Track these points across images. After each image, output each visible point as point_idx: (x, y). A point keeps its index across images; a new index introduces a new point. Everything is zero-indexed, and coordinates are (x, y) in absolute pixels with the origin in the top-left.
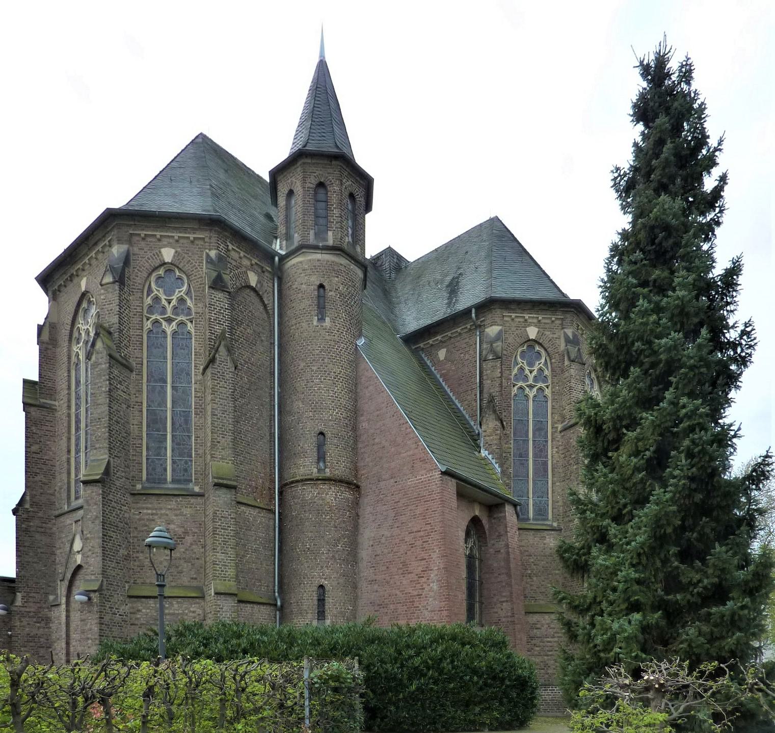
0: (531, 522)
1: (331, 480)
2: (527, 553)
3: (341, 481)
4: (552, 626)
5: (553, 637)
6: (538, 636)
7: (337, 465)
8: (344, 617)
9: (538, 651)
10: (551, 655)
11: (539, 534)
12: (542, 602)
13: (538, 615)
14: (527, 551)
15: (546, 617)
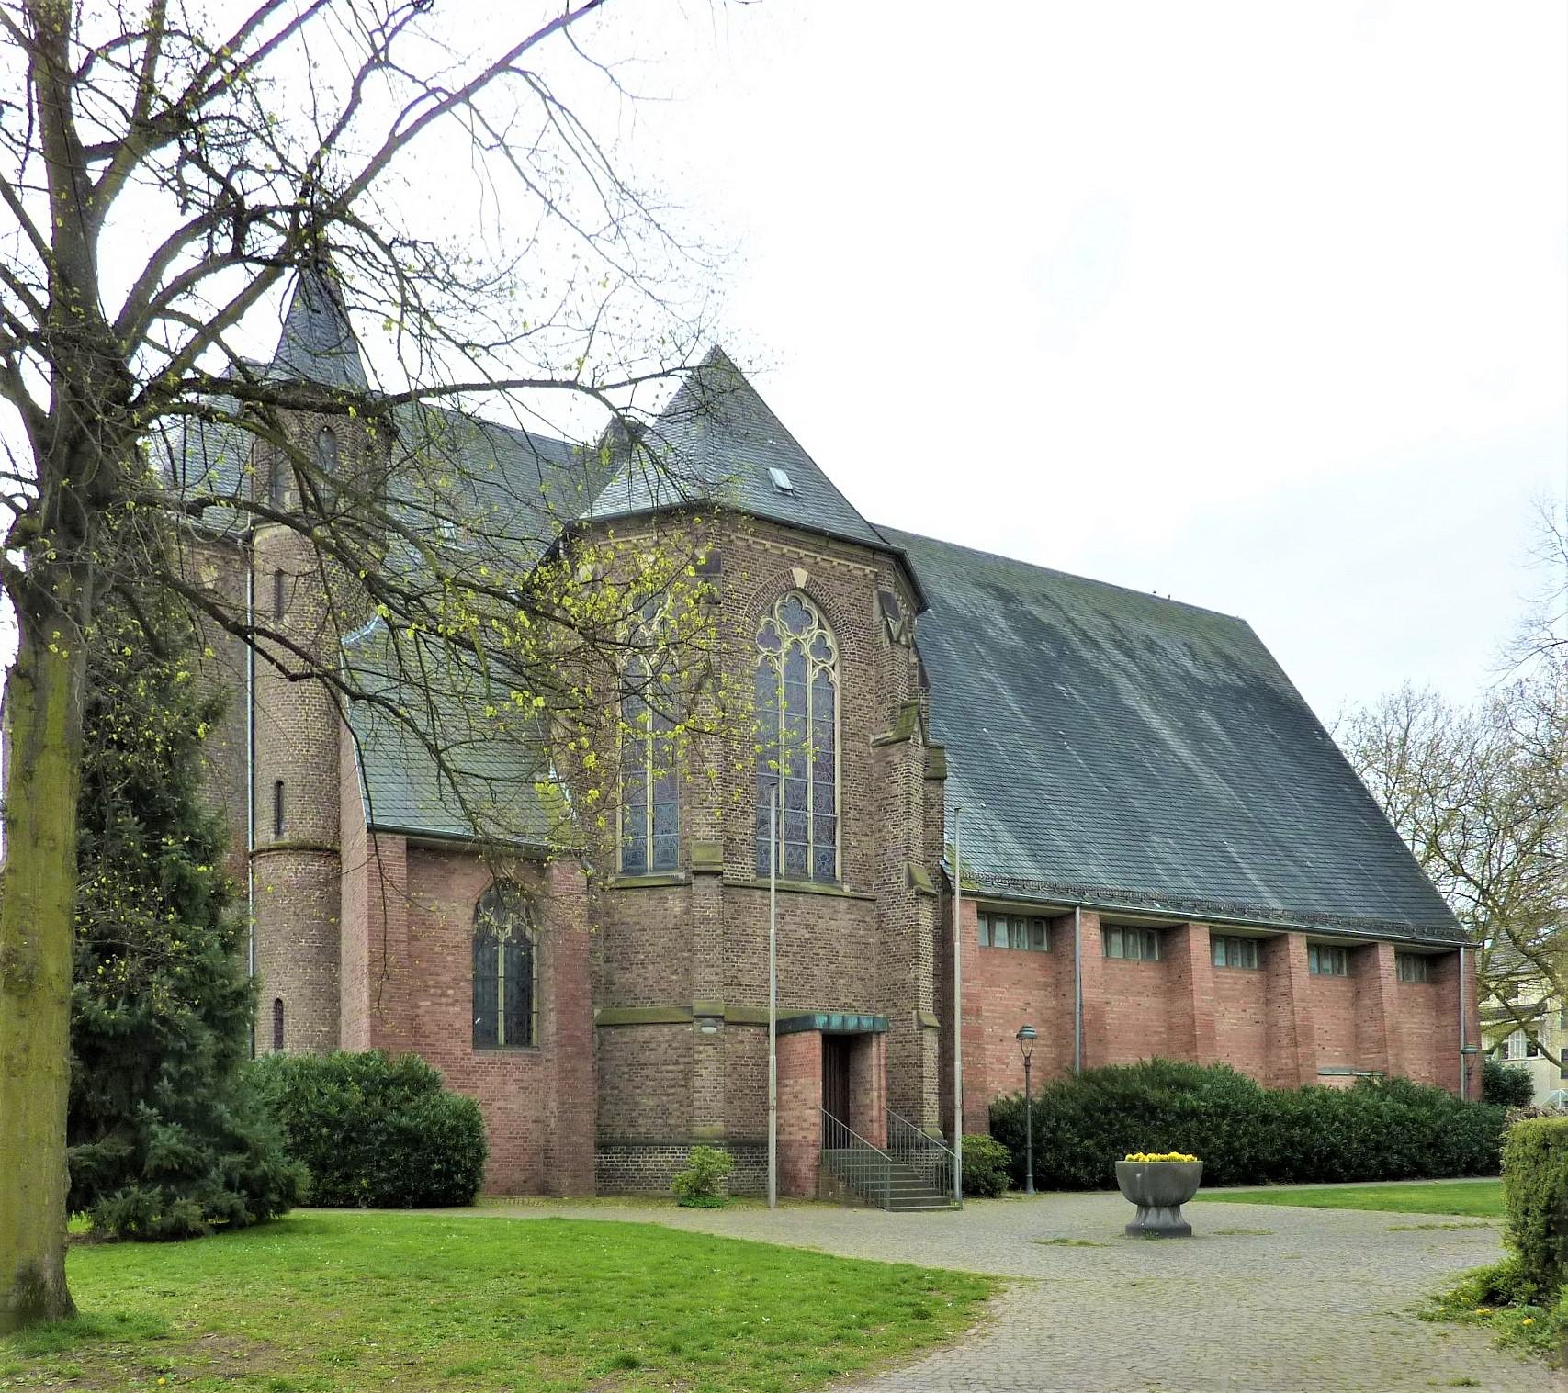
0: (649, 874)
1: (287, 848)
2: (638, 927)
3: (315, 849)
4: (675, 1045)
5: (677, 1063)
6: (653, 1062)
7: (303, 825)
8: (311, 1042)
9: (652, 1087)
10: (673, 1094)
11: (657, 893)
12: (662, 1006)
13: (652, 1027)
14: (638, 923)
15: (666, 1030)
